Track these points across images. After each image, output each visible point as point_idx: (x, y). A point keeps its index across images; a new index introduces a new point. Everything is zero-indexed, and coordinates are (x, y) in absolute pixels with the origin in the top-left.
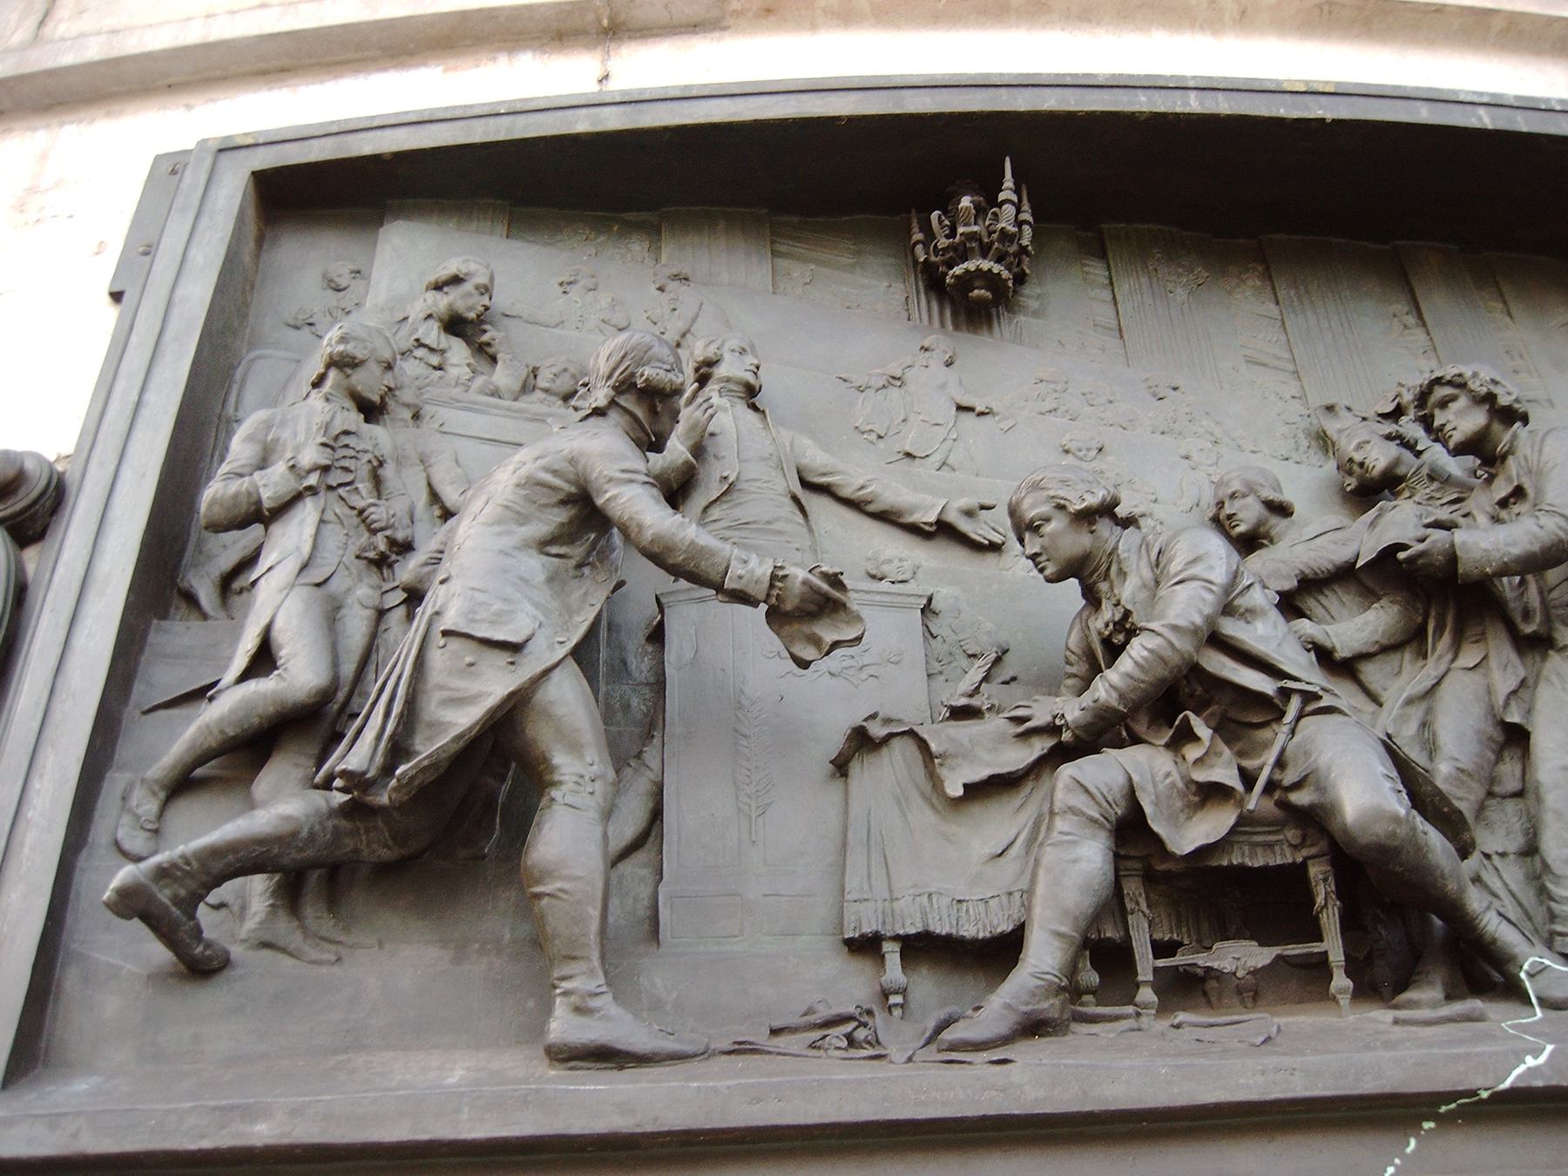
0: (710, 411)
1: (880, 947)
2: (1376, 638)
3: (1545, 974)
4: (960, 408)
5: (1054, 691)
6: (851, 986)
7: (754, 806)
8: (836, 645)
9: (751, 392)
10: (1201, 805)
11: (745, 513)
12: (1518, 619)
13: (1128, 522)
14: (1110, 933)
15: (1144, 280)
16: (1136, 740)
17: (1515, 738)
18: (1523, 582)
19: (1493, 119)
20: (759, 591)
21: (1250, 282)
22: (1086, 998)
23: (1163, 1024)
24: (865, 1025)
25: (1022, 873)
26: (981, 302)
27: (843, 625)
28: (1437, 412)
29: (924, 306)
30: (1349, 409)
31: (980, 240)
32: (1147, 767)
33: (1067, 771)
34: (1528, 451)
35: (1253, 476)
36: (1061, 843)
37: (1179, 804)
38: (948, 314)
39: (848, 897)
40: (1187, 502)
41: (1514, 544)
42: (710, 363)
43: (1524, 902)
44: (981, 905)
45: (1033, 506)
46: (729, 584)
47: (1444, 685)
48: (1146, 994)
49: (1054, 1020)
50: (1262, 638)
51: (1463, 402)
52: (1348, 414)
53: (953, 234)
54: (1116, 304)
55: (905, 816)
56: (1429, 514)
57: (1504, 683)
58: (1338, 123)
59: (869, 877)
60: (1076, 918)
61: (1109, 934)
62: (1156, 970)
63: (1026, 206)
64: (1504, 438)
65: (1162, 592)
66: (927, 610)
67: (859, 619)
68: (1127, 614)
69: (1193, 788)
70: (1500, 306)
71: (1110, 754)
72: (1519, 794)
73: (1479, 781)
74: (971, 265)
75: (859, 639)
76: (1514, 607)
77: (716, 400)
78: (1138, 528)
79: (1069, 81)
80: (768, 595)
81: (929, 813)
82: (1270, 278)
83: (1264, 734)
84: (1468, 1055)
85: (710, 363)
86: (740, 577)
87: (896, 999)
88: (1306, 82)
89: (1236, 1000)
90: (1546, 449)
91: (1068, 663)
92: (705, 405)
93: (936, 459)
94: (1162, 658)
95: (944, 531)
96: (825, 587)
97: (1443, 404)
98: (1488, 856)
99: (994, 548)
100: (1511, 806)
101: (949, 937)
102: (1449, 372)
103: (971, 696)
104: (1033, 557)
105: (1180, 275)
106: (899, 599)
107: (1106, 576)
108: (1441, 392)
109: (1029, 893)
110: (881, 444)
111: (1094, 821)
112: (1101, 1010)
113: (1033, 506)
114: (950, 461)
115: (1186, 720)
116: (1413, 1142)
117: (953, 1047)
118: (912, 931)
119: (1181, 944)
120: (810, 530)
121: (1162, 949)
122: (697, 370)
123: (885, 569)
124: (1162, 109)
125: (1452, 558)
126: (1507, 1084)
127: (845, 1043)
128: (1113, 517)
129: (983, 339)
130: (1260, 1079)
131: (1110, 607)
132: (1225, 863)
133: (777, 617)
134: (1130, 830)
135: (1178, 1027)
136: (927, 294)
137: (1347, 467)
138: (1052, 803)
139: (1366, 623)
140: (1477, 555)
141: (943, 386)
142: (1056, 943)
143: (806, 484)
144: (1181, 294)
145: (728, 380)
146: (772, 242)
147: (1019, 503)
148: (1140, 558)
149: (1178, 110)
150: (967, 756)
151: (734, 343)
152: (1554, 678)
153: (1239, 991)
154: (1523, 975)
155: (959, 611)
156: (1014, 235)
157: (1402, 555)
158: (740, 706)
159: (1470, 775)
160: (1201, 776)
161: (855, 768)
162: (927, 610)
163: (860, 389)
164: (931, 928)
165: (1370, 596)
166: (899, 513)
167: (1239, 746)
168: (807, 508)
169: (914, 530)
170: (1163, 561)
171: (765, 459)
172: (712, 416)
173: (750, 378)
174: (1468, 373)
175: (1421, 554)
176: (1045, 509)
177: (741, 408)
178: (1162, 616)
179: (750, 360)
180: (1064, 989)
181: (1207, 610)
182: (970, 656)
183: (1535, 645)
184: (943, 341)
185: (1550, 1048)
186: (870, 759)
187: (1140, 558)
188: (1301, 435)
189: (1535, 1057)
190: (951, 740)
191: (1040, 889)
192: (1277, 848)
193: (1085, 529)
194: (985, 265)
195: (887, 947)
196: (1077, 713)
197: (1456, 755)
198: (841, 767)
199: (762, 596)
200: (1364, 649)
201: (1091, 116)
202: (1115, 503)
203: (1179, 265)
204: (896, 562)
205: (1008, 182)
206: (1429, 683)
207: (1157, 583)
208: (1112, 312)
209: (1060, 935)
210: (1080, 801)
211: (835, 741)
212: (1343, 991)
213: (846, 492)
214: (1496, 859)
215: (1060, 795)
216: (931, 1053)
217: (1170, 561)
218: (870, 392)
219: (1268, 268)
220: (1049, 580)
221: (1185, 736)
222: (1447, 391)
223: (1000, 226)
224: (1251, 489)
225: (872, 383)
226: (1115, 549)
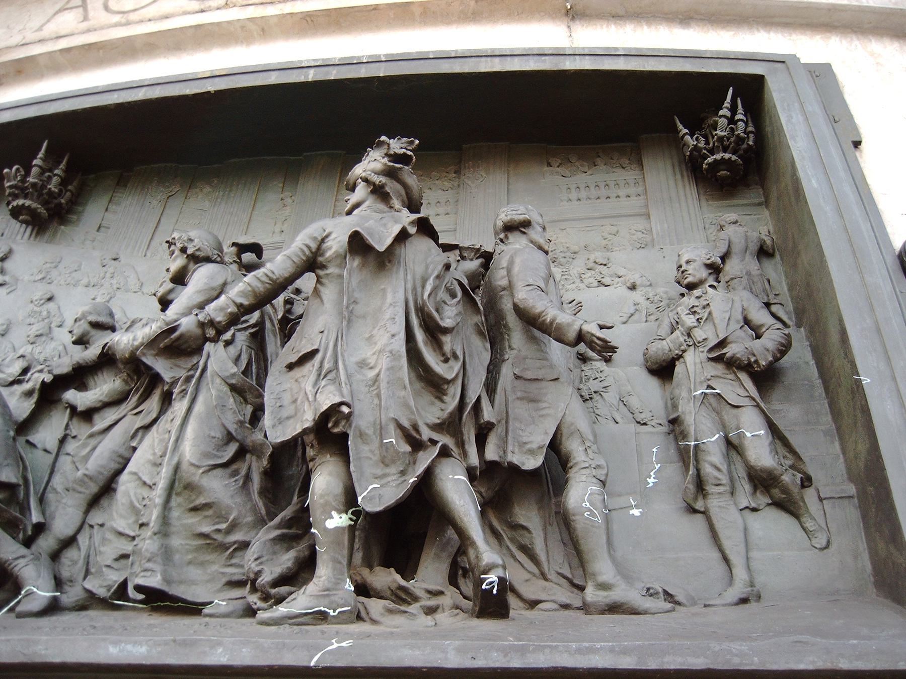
2: (101, 398)
21: (205, 191)
58: (219, 93)
98: (91, 526)
140: (122, 346)
200: (93, 405)
214: (96, 527)
224: (84, 316)
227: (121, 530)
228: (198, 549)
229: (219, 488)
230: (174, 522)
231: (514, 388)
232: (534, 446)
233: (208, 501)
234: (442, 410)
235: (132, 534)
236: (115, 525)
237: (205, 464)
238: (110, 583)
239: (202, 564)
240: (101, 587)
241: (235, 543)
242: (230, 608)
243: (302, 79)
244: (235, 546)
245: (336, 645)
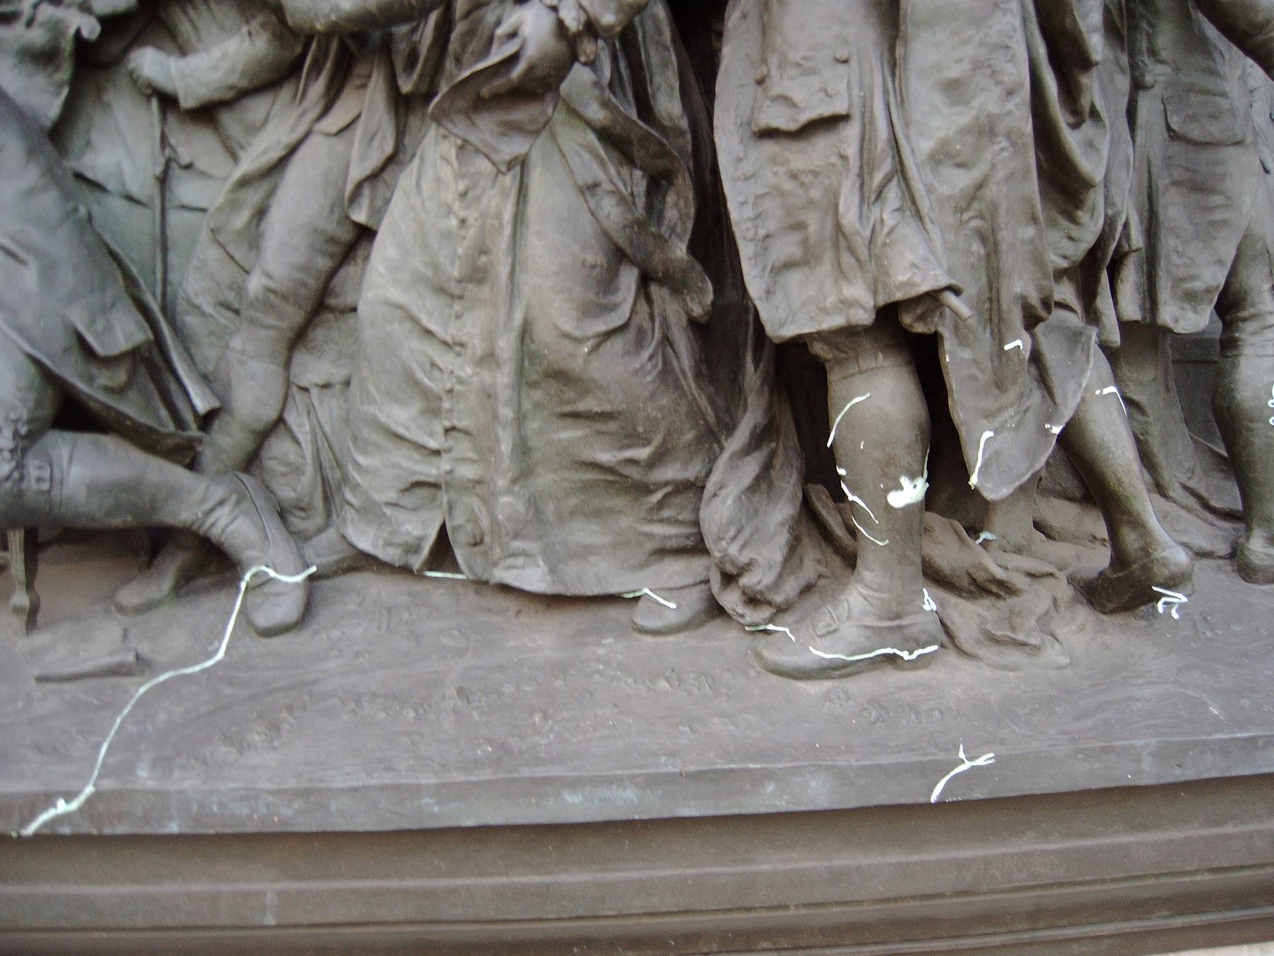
17: (365, 234)
73: (296, 303)
98: (306, 390)
139: (224, 56)
159: (284, 297)
200: (216, 96)
206: (275, 155)
214: (314, 391)
228: (585, 488)
229: (622, 374)
230: (534, 442)
231: (1167, 160)
232: (1198, 285)
233: (607, 407)
234: (1071, 238)
235: (433, 444)
236: (382, 418)
237: (590, 332)
238: (410, 540)
239: (598, 514)
240: (388, 544)
241: (667, 484)
242: (686, 614)
244: (668, 489)
245: (967, 765)
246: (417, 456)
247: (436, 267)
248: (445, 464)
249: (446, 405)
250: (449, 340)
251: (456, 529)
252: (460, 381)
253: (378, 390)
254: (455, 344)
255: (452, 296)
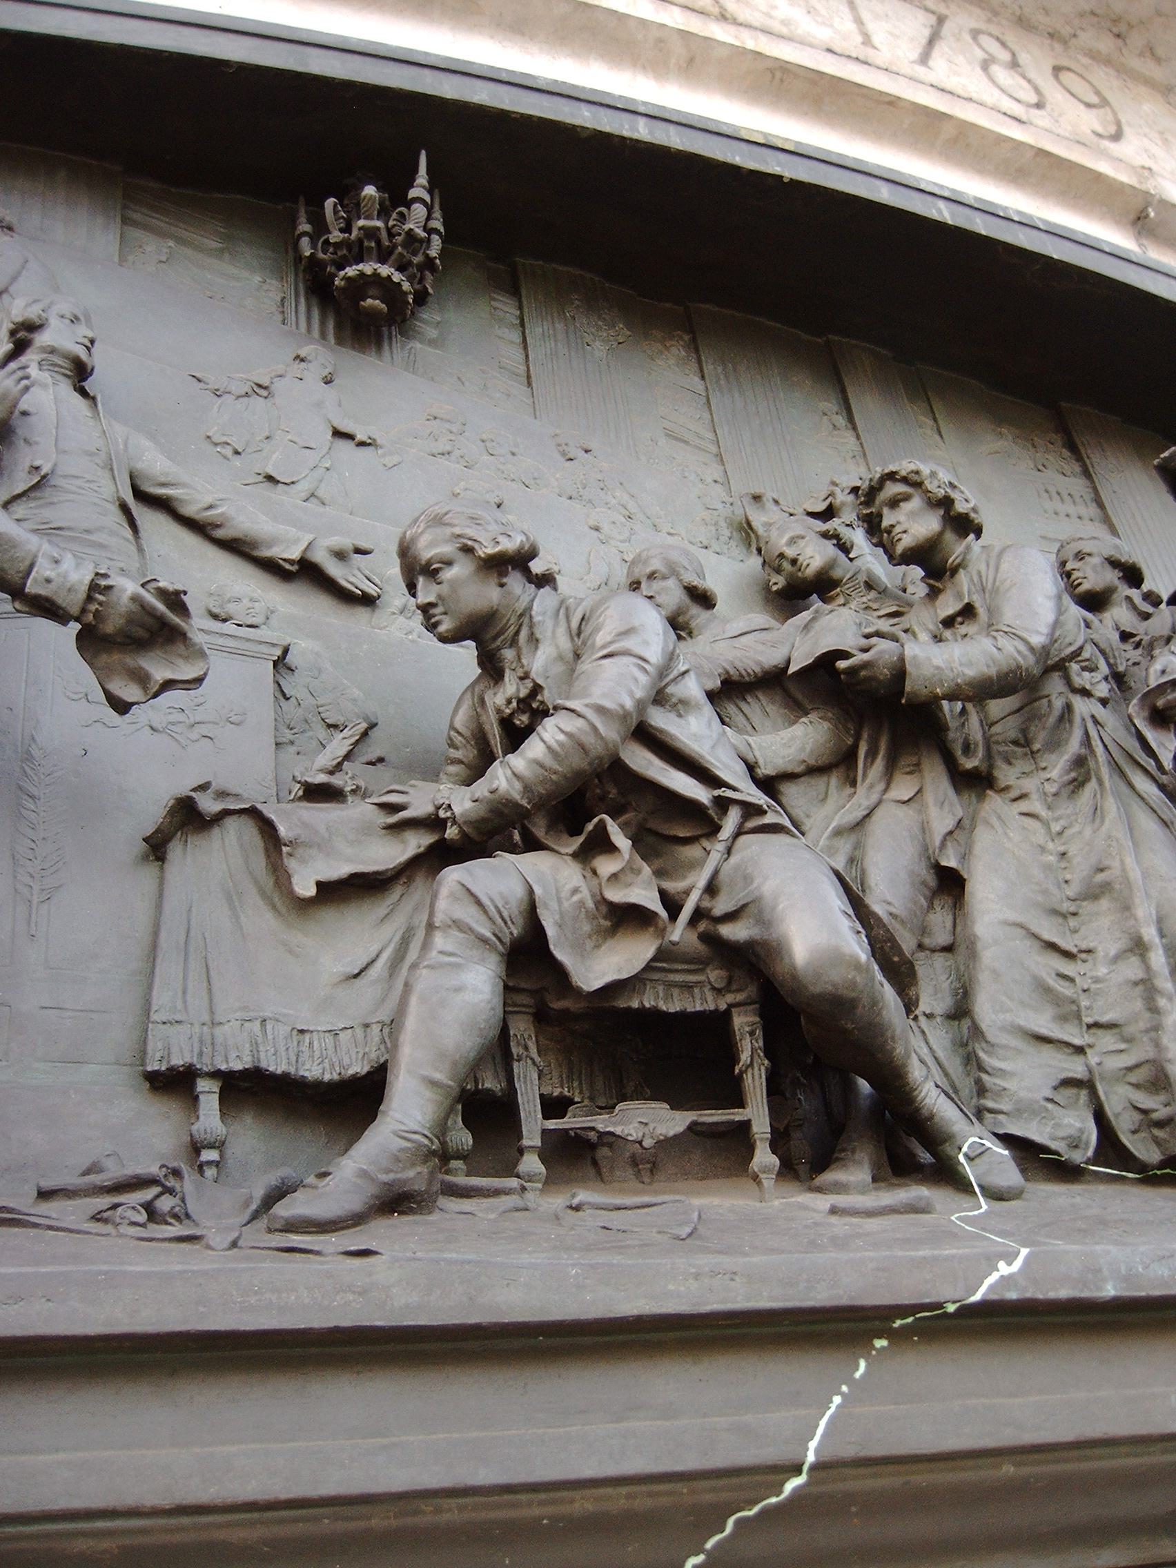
0: (25, 382)
1: (192, 1085)
2: (803, 756)
3: (985, 1157)
4: (338, 434)
5: (431, 774)
6: (147, 1136)
7: (36, 888)
8: (168, 685)
9: (80, 373)
10: (613, 931)
11: (56, 516)
12: (959, 753)
13: (545, 581)
14: (491, 1083)
15: (559, 326)
16: (532, 844)
18: (964, 711)
19: (952, 214)
20: (73, 602)
21: (674, 350)
22: (455, 1164)
23: (556, 1201)
24: (170, 1191)
25: (383, 1000)
26: (373, 314)
27: (180, 662)
28: (886, 511)
29: (301, 311)
30: (776, 502)
31: (379, 242)
32: (550, 878)
33: (453, 875)
34: (983, 568)
35: (675, 556)
36: (442, 966)
37: (587, 928)
38: (331, 325)
39: (154, 1017)
40: (595, 579)
41: (970, 664)
42: (32, 327)
43: (951, 1071)
44: (329, 1039)
45: (432, 544)
46: (30, 588)
47: (876, 817)
48: (531, 1163)
49: (420, 1193)
50: (696, 737)
51: (916, 503)
52: (775, 508)
53: (347, 229)
54: (525, 348)
55: (237, 918)
56: (869, 624)
57: (941, 822)
58: (796, 184)
59: (184, 993)
60: (455, 1063)
61: (488, 1085)
62: (545, 1132)
63: (437, 214)
64: (956, 548)
65: (585, 666)
66: (280, 663)
67: (202, 654)
68: (536, 689)
69: (604, 909)
70: (931, 423)
71: (505, 859)
72: (949, 949)
73: (911, 930)
74: (368, 268)
75: (199, 681)
76: (955, 738)
77: (33, 371)
78: (555, 589)
79: (504, 77)
80: (84, 611)
81: (269, 915)
82: (697, 351)
83: (693, 851)
84: (935, 1259)
85: (32, 327)
86: (48, 581)
87: (209, 1155)
88: (765, 135)
89: (630, 1172)
90: (1004, 566)
91: (452, 745)
92: (20, 374)
93: (303, 487)
94: (582, 746)
95: (307, 572)
96: (161, 607)
97: (894, 503)
99: (367, 601)
100: (940, 960)
101: (285, 1076)
102: (904, 467)
103: (331, 773)
104: (426, 609)
105: (599, 329)
106: (247, 646)
107: (514, 642)
108: (892, 489)
109: (393, 1026)
110: (237, 461)
111: (484, 940)
112: (476, 1181)
113: (432, 544)
114: (320, 493)
115: (602, 826)
116: (862, 1364)
117: (292, 1226)
118: (237, 1066)
119: (571, 1102)
120: (140, 550)
121: (553, 1107)
122: (13, 333)
123: (231, 608)
124: (607, 129)
125: (900, 673)
126: (977, 1297)
127: (142, 1217)
128: (527, 572)
129: (370, 359)
130: (694, 1285)
131: (515, 681)
132: (635, 1004)
133: (93, 641)
134: (527, 955)
135: (577, 1208)
136: (307, 299)
137: (774, 563)
138: (432, 914)
139: (793, 738)
140: (927, 671)
141: (319, 405)
142: (428, 1094)
143: (139, 495)
144: (599, 349)
145: (53, 351)
146: (124, 207)
147: (414, 540)
148: (556, 625)
149: (626, 133)
150: (323, 846)
151: (65, 306)
152: (994, 821)
153: (634, 1162)
154: (961, 1158)
155: (320, 671)
156: (421, 241)
157: (842, 664)
158: (29, 757)
159: (903, 922)
160: (616, 895)
161: (175, 850)
162: (280, 663)
163: (217, 394)
164: (263, 1065)
165: (797, 709)
166: (254, 544)
167: (658, 863)
168: (139, 523)
169: (271, 567)
170: (587, 630)
171: (91, 454)
172: (27, 388)
173: (83, 354)
174: (925, 470)
175: (866, 665)
176: (447, 549)
177: (65, 389)
178: (584, 693)
179: (83, 331)
180: (433, 1153)
181: (639, 694)
182: (329, 726)
183: (974, 783)
184: (322, 355)
185: (1024, 1252)
186: (195, 841)
187: (556, 625)
188: (724, 524)
189: (1009, 1264)
190: (305, 825)
191: (411, 1022)
192: (696, 991)
193: (493, 580)
194: (385, 270)
195: (202, 1085)
196: (468, 805)
197: (889, 899)
198: (157, 847)
199: (75, 610)
200: (790, 768)
201: (527, 120)
202: (532, 554)
203: (600, 317)
204: (245, 601)
205: (422, 178)
206: (860, 814)
207: (577, 656)
208: (520, 356)
209: (433, 1084)
210: (469, 914)
211: (152, 812)
212: (766, 1170)
213: (189, 510)
215: (442, 904)
216: (257, 1235)
217: (597, 629)
218: (228, 399)
219: (694, 340)
220: (444, 639)
221: (600, 844)
222: (900, 488)
223: (406, 227)
225: (233, 388)
226: (529, 608)
227: (1044, 1031)
235: (1077, 1041)
238: (1072, 1132)
243: (933, 214)
246: (1059, 1056)
247: (1045, 892)
248: (1093, 1058)
249: (1084, 1003)
250: (1075, 950)
251: (1117, 1115)
252: (1097, 980)
253: (1011, 999)
254: (1081, 951)
255: (1064, 916)
